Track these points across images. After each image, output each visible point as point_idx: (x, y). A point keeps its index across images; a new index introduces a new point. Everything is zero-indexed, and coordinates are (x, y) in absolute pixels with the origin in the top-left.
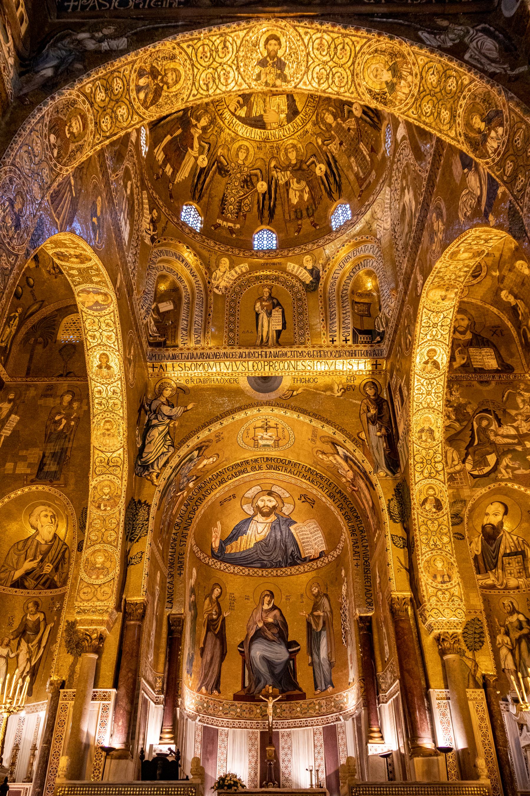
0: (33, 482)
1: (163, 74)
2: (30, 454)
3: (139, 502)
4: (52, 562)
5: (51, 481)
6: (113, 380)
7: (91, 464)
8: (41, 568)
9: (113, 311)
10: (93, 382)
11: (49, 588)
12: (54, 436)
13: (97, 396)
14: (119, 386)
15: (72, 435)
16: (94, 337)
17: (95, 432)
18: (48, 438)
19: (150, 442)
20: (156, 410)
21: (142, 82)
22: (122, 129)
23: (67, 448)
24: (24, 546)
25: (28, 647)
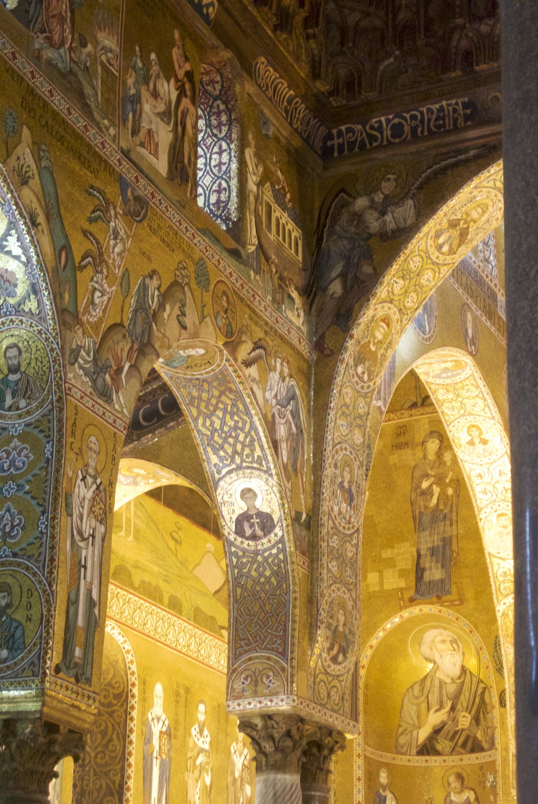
1: (465, 216)
2: (399, 554)
4: (468, 710)
5: (439, 597)
7: (492, 579)
8: (454, 720)
9: (472, 375)
11: (472, 751)
12: (426, 519)
15: (454, 514)
16: (453, 408)
21: (441, 240)
22: (431, 289)
23: (451, 537)
24: (422, 690)
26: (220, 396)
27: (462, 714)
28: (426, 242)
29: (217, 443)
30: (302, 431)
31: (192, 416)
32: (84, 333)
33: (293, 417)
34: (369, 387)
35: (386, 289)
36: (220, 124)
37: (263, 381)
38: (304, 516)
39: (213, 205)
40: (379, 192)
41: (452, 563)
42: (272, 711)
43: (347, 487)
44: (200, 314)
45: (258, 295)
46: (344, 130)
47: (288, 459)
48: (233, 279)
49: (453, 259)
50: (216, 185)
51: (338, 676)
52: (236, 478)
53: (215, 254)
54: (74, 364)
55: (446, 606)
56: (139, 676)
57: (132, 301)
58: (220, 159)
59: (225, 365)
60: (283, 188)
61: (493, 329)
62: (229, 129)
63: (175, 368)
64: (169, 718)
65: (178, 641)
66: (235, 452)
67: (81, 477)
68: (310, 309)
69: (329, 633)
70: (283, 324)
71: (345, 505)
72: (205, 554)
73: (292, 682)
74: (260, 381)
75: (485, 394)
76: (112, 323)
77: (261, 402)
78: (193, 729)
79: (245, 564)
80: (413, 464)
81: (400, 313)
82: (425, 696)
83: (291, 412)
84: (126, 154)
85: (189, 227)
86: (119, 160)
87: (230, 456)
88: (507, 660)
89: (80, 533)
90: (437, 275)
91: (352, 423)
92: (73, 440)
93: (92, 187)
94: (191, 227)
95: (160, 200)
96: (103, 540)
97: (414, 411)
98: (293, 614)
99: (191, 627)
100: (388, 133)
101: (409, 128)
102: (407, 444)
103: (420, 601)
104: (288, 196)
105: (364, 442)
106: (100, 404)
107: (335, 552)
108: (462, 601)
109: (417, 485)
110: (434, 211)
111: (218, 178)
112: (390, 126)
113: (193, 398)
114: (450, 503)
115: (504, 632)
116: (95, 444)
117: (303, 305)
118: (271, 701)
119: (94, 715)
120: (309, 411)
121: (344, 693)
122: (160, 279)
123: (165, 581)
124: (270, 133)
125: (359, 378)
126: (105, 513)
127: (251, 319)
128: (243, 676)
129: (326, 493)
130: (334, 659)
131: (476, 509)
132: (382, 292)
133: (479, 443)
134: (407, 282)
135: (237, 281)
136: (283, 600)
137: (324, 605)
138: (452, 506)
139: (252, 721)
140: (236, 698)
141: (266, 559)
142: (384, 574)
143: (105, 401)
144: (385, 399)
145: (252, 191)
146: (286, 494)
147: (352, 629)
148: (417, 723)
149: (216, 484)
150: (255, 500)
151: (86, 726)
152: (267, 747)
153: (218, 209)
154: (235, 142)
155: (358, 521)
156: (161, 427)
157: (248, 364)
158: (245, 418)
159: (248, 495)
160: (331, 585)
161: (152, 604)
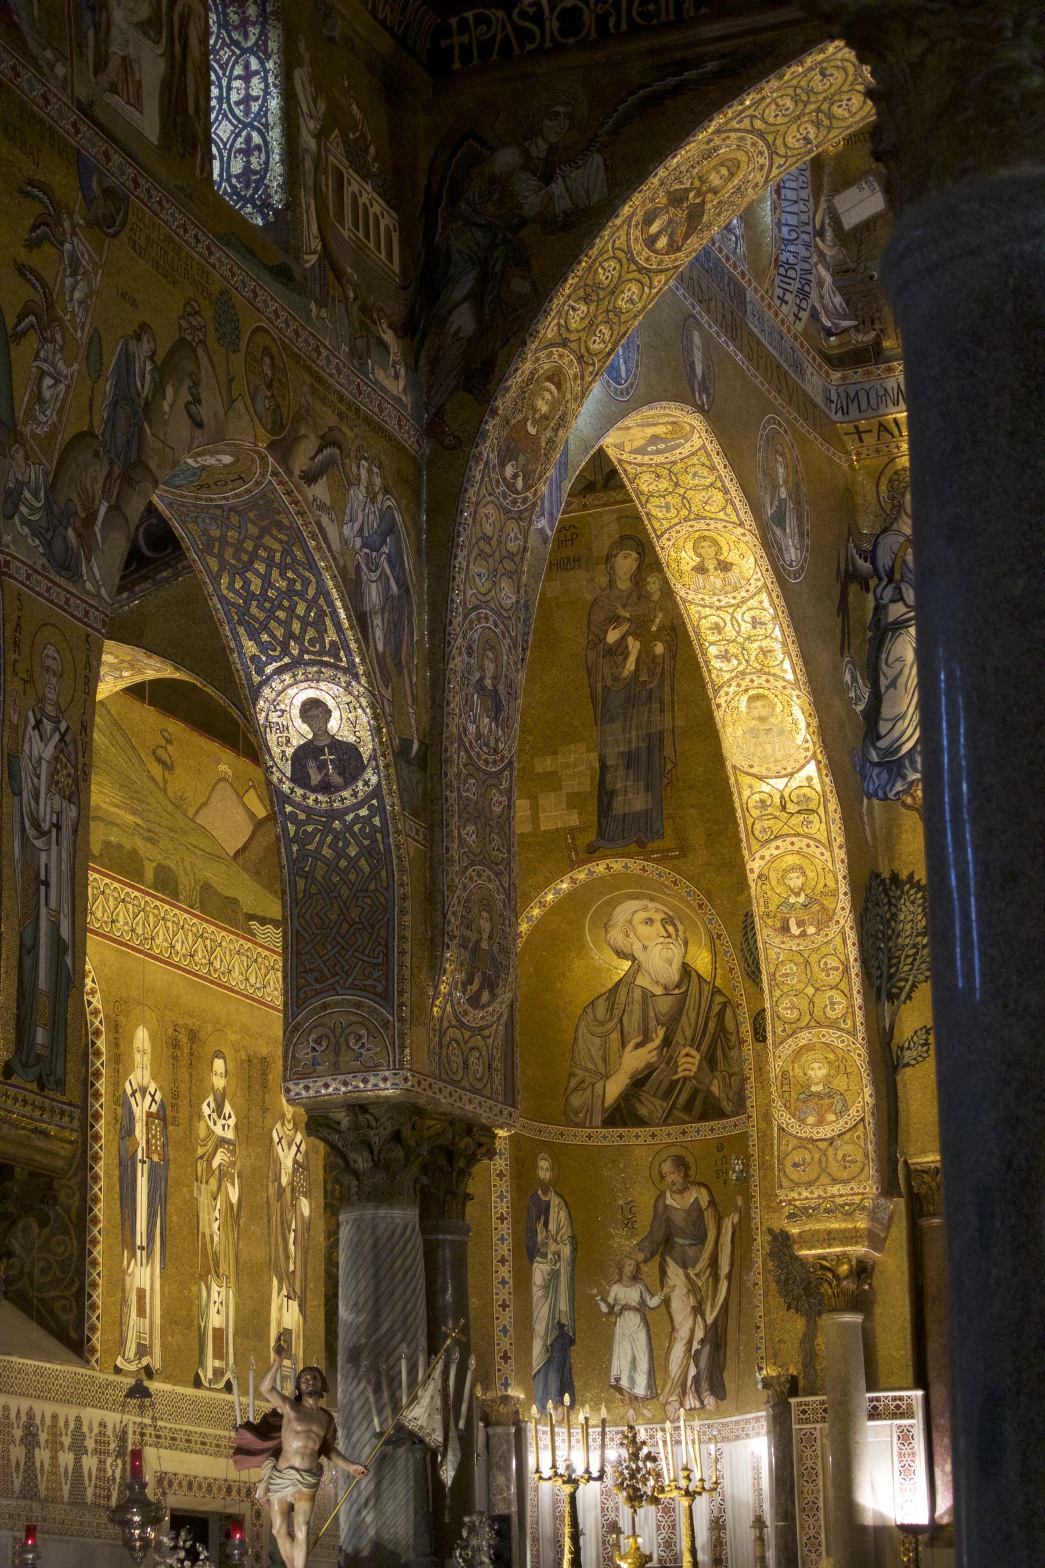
0: (593, 852)
1: (697, 184)
2: (566, 766)
3: (895, 878)
5: (642, 845)
6: (744, 594)
7: (739, 814)
8: (671, 1062)
10: (693, 609)
11: (703, 1117)
13: (712, 638)
14: (766, 604)
15: (667, 689)
17: (729, 730)
18: (604, 712)
19: (893, 684)
20: (892, 569)
21: (654, 228)
23: (661, 733)
24: (611, 1009)
25: (687, 1276)
26: (260, 537)
27: (683, 1052)
28: (628, 234)
29: (256, 619)
30: (407, 591)
31: (209, 571)
32: (27, 458)
33: (392, 567)
34: (525, 500)
35: (555, 322)
36: (244, 24)
37: (338, 509)
38: (416, 746)
39: (237, 177)
40: (539, 140)
41: (665, 781)
42: (368, 1098)
43: (490, 687)
44: (225, 395)
45: (325, 346)
46: (471, 20)
47: (385, 645)
48: (280, 323)
49: (676, 260)
50: (240, 140)
51: (481, 1029)
52: (292, 681)
53: (247, 279)
54: (11, 517)
55: (653, 861)
56: (107, 1016)
57: (108, 387)
58: (247, 88)
59: (270, 482)
60: (363, 135)
61: (739, 357)
62: (263, 33)
63: (178, 487)
64: (161, 1088)
65: (172, 947)
66: (290, 635)
67: (33, 722)
68: (417, 360)
69: (465, 955)
70: (369, 395)
71: (487, 720)
72: (216, 784)
73: (402, 1048)
74: (332, 507)
75: (727, 481)
76: (75, 432)
77: (336, 545)
78: (205, 1106)
79: (311, 836)
80: (589, 597)
81: (579, 363)
82: (616, 1020)
83: (389, 556)
84: (85, 109)
85: (200, 234)
86: (74, 125)
87: (280, 643)
88: (766, 959)
89: (36, 824)
90: (647, 290)
91: (496, 570)
92: (16, 656)
93: (30, 182)
94: (204, 234)
95: (148, 191)
96: (75, 832)
97: (590, 499)
98: (400, 925)
99: (195, 920)
100: (553, 25)
101: (593, 15)
102: (577, 560)
103: (608, 852)
104: (372, 150)
105: (518, 602)
106: (60, 586)
107: (471, 808)
108: (683, 852)
109: (597, 636)
110: (641, 176)
111: (245, 126)
112: (556, 14)
113: (211, 540)
114: (659, 670)
115: (762, 909)
116: (54, 659)
117: (404, 355)
118: (365, 1081)
119: (71, 1142)
120: (419, 551)
121: (492, 1058)
122: (155, 340)
123: (149, 840)
124: (337, 34)
125: (508, 486)
126: (76, 782)
127: (314, 393)
128: (314, 1036)
129: (455, 703)
130: (474, 1001)
131: (709, 686)
132: (549, 328)
133: (716, 569)
134: (593, 307)
135: (288, 326)
136: (382, 899)
137: (455, 907)
138: (662, 675)
139: (330, 1115)
140: (303, 1076)
141: (349, 828)
142: (540, 802)
143: (68, 579)
144: (551, 515)
145: (307, 150)
146: (383, 709)
147: (504, 943)
148: (602, 1070)
149: (256, 693)
150: (327, 720)
151: (60, 1163)
152: (360, 1161)
153: (247, 186)
154: (275, 57)
155: (510, 747)
156: (145, 578)
157: (310, 478)
158: (307, 574)
159: (314, 712)
160: (466, 868)
161: (125, 884)
